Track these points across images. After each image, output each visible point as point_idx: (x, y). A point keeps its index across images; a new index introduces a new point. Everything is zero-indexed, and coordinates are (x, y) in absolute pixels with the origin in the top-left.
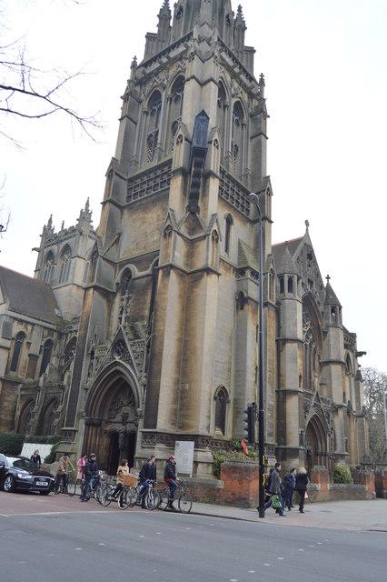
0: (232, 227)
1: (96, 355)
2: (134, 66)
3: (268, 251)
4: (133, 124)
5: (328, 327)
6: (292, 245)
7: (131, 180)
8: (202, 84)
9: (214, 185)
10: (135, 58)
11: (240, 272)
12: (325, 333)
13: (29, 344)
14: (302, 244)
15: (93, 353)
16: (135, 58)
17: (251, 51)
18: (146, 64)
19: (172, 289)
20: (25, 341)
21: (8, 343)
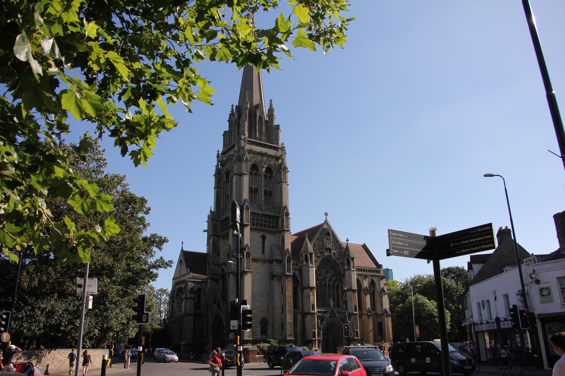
0: (266, 241)
1: (213, 309)
2: (218, 156)
3: (288, 246)
4: (220, 189)
5: (345, 270)
6: (312, 232)
7: (222, 221)
8: (241, 175)
9: (247, 230)
10: (218, 151)
11: (271, 262)
12: (344, 275)
13: (204, 294)
14: (320, 230)
15: (212, 308)
16: (218, 151)
17: (278, 127)
18: (224, 153)
19: (232, 280)
20: (202, 292)
21: (193, 296)
